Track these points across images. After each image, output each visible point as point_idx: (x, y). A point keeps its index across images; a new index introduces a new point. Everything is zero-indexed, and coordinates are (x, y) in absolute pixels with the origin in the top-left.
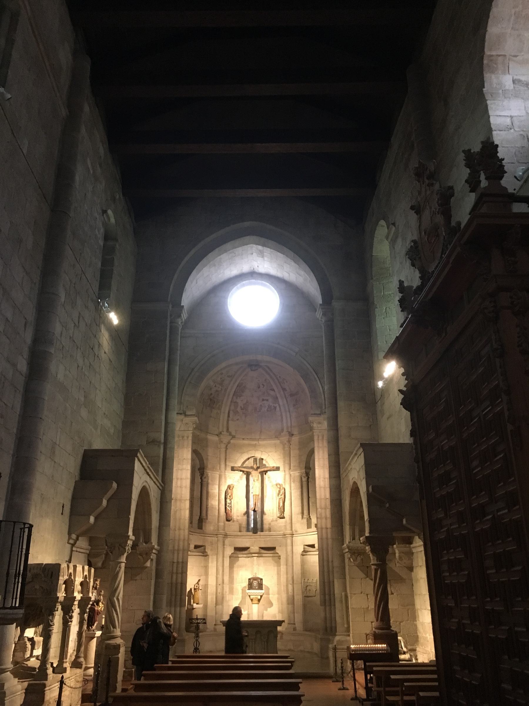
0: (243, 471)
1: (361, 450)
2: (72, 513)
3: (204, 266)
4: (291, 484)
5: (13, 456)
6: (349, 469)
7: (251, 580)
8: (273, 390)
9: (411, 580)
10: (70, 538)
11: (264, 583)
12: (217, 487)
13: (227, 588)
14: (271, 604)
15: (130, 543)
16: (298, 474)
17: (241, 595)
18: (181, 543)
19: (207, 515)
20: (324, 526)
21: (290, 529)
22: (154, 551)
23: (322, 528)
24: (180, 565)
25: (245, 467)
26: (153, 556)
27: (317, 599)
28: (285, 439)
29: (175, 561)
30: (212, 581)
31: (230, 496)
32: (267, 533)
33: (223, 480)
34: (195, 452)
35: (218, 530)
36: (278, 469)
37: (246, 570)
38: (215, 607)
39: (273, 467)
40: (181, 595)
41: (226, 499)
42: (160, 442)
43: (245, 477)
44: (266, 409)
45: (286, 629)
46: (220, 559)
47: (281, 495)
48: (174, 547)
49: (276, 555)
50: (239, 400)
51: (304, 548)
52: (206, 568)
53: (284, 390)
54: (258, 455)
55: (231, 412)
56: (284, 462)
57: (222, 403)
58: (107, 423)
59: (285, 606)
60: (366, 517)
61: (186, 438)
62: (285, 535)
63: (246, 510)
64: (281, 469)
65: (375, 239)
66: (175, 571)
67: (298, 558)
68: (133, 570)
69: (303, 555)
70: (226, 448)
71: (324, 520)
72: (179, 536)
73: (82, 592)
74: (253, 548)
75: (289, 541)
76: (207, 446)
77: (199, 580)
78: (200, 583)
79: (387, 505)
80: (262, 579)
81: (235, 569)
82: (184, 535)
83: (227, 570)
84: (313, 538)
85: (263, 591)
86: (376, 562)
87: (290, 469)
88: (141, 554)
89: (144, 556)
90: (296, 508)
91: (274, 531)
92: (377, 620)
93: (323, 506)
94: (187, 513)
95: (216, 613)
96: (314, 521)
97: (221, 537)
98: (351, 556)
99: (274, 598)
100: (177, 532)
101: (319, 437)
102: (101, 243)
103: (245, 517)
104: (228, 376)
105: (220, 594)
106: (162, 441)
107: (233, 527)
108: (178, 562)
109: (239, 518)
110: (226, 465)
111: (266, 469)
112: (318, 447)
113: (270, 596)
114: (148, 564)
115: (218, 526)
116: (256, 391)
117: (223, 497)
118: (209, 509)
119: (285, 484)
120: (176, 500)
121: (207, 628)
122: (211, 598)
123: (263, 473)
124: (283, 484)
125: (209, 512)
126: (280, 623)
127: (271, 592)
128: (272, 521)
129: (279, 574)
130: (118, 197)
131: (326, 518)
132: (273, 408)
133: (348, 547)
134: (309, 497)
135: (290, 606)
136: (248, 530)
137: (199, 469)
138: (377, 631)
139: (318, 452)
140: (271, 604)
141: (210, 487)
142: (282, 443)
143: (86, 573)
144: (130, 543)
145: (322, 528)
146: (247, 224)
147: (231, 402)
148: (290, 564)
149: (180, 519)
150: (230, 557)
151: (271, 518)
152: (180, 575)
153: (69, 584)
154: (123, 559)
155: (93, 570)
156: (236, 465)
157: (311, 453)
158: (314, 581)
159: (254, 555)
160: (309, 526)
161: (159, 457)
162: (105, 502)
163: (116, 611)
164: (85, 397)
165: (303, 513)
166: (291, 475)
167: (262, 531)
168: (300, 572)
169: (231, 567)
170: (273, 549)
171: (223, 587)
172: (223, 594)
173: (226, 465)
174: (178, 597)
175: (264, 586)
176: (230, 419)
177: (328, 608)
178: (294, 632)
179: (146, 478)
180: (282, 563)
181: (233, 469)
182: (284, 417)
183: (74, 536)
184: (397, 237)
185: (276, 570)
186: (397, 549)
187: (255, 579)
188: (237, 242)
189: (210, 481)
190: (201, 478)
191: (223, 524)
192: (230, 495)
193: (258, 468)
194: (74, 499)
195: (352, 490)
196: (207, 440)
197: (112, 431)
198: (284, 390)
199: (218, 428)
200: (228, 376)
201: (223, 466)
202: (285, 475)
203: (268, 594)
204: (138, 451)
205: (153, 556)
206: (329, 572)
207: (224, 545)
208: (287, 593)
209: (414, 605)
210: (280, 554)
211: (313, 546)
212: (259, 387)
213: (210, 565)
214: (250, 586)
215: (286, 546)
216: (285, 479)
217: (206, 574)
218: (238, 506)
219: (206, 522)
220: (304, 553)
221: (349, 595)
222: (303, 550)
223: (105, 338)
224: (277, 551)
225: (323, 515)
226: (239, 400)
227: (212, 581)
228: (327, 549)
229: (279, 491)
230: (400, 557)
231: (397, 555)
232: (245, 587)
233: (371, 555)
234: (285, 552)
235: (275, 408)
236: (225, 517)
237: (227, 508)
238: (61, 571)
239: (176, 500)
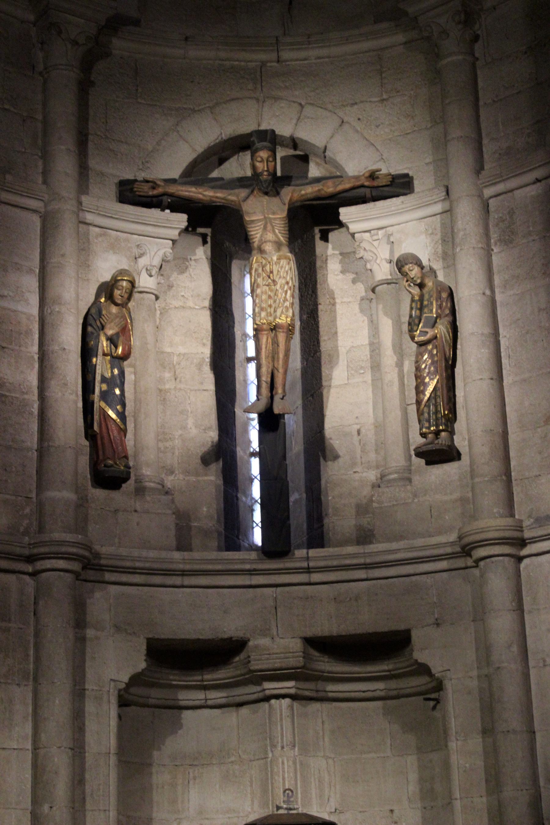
12: (31, 283)
16: (533, 191)
33: (66, 244)
35: (41, 529)
36: (400, 185)
39: (373, 176)
41: (87, 352)
43: (201, 257)
46: (58, 706)
47: (434, 325)
49: (418, 682)
63: (213, 435)
70: (84, 87)
74: (264, 642)
75: (497, 582)
81: (160, 777)
87: (479, 168)
97: (60, 584)
103: (212, 477)
107: (132, 529)
109: (169, 481)
110: (83, 170)
115: (40, 505)
117: (69, 336)
123: (314, 220)
124: (437, 266)
128: (376, 486)
151: (372, 475)
159: (271, 687)
166: (486, 208)
167: (317, 538)
169: (135, 760)
173: (83, 170)
180: (453, 724)
185: (413, 776)
201: (65, 164)
207: (80, 623)
210: (436, 669)
224: (420, 656)
229: (420, 305)
234: (471, 655)
236: (84, 461)
237: (98, 403)
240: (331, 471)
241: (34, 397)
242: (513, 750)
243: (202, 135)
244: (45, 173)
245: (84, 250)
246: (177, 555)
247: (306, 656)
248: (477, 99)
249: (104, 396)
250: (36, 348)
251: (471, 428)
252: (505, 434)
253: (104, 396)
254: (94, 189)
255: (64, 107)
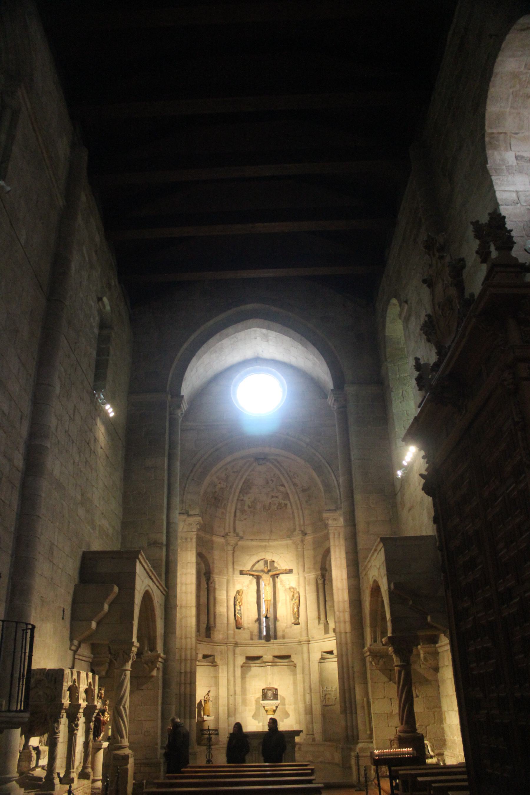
0: (253, 575)
1: (381, 545)
2: (74, 618)
3: (205, 353)
4: (305, 587)
5: (12, 556)
6: (369, 567)
7: (265, 691)
8: (283, 485)
9: (437, 681)
10: (72, 644)
11: (279, 693)
12: (225, 592)
13: (239, 699)
14: (287, 715)
15: (134, 649)
16: (313, 576)
17: (255, 707)
18: (189, 653)
19: (215, 623)
20: (343, 631)
21: (306, 635)
22: (160, 660)
23: (340, 633)
24: (189, 676)
25: (254, 571)
26: (159, 665)
27: (337, 708)
28: (298, 538)
29: (183, 671)
30: (223, 692)
31: (239, 603)
32: (281, 640)
33: (231, 585)
34: (200, 555)
35: (228, 639)
36: (291, 571)
37: (260, 679)
38: (228, 719)
39: (286, 570)
40: (190, 707)
41: (235, 605)
42: (162, 544)
43: (255, 581)
44: (276, 507)
45: (304, 740)
47: (296, 599)
48: (181, 656)
49: (292, 663)
50: (246, 498)
51: (322, 655)
52: (216, 677)
53: (295, 485)
54: (269, 557)
55: (238, 511)
56: (298, 563)
57: (228, 502)
58: (105, 523)
59: (303, 717)
60: (388, 616)
61: (189, 540)
62: (300, 642)
63: (257, 617)
64: (294, 571)
65: (388, 319)
66: (183, 681)
67: (315, 666)
68: (139, 680)
69: (320, 662)
70: (234, 551)
71: (342, 625)
72: (186, 644)
73: (87, 700)
75: (305, 648)
76: (212, 548)
77: (209, 691)
78: (210, 694)
79: (411, 603)
80: (276, 689)
81: (247, 679)
82: (191, 644)
83: (239, 680)
84: (331, 644)
85: (278, 702)
86: (399, 663)
87: (304, 571)
88: (146, 663)
89: (150, 664)
90: (312, 613)
91: (289, 638)
92: (402, 724)
93: (341, 609)
94: (193, 621)
95: (228, 726)
96: (332, 625)
98: (373, 660)
99: (290, 708)
100: (184, 641)
101: (334, 535)
102: (96, 331)
103: (257, 625)
104: (234, 472)
105: (233, 705)
106: (165, 542)
107: (243, 635)
108: (186, 672)
109: (249, 626)
111: (277, 572)
112: (335, 545)
113: (286, 706)
114: (154, 673)
115: (227, 634)
116: (264, 488)
118: (217, 616)
119: (299, 588)
120: (181, 607)
121: (219, 741)
122: (223, 710)
123: (275, 577)
124: (297, 587)
125: (217, 620)
126: (297, 733)
127: (287, 702)
128: (286, 628)
129: (295, 683)
130: (113, 284)
131: (345, 622)
132: (283, 505)
133: (369, 650)
134: (325, 601)
135: (308, 717)
136: (260, 638)
137: (205, 574)
138: (402, 735)
139: (335, 552)
140: (287, 715)
141: (217, 592)
142: (294, 543)
143: (90, 680)
144: (134, 649)
145: (340, 633)
146: (249, 307)
147: (238, 500)
148: (306, 671)
149: (186, 627)
150: (242, 667)
151: (285, 625)
152: (188, 686)
153: (73, 690)
154: (128, 666)
155: (97, 677)
156: (245, 569)
157: (327, 552)
158: (333, 690)
159: (267, 664)
160: (326, 631)
161: (161, 560)
162: (106, 607)
163: (123, 720)
164: (82, 495)
165: (319, 618)
166: (305, 578)
167: (275, 638)
168: (318, 680)
170: (288, 657)
171: (235, 699)
172: (235, 705)
174: (188, 709)
175: (279, 697)
176: (237, 519)
177: (349, 716)
178: (313, 743)
179: (148, 581)
181: (242, 573)
182: (296, 515)
183: (76, 642)
184: (410, 315)
185: (292, 680)
186: (421, 650)
187: (269, 689)
188: (240, 326)
189: (217, 586)
190: (207, 584)
191: (232, 632)
192: (239, 601)
193: (269, 571)
194: (74, 602)
195: (372, 589)
196: (212, 542)
197: (111, 531)
198: (295, 485)
199: (225, 529)
200: (234, 472)
201: (231, 570)
202: (299, 578)
203: (284, 704)
204: (138, 552)
205: (159, 665)
206: (349, 678)
207: (234, 654)
208: (305, 703)
209: (440, 707)
210: (295, 662)
211: (331, 653)
212: (268, 483)
213: (220, 675)
214: (265, 696)
215: (302, 653)
216: (299, 583)
217: (217, 684)
218: (249, 613)
219: (214, 630)
220: (322, 661)
221: (371, 701)
222: (320, 657)
223: (101, 431)
225: (342, 619)
226: (246, 498)
227: (223, 692)
228: (347, 655)
229: (293, 596)
230: (425, 659)
231: (422, 656)
232: (259, 698)
233: (394, 657)
235: (286, 505)
236: (235, 624)
237: (237, 615)
238: (65, 677)
239: (181, 607)
240: (278, 624)
241: (226, 614)
242: (307, 677)
243: (255, 559)
244: (227, 571)
245: (234, 584)
246: (251, 641)
247: (273, 659)
248: (304, 556)
249: (238, 613)
250: (226, 605)
251: (302, 619)
252: (307, 622)
253: (238, 613)
254: (236, 572)
255: (230, 559)
